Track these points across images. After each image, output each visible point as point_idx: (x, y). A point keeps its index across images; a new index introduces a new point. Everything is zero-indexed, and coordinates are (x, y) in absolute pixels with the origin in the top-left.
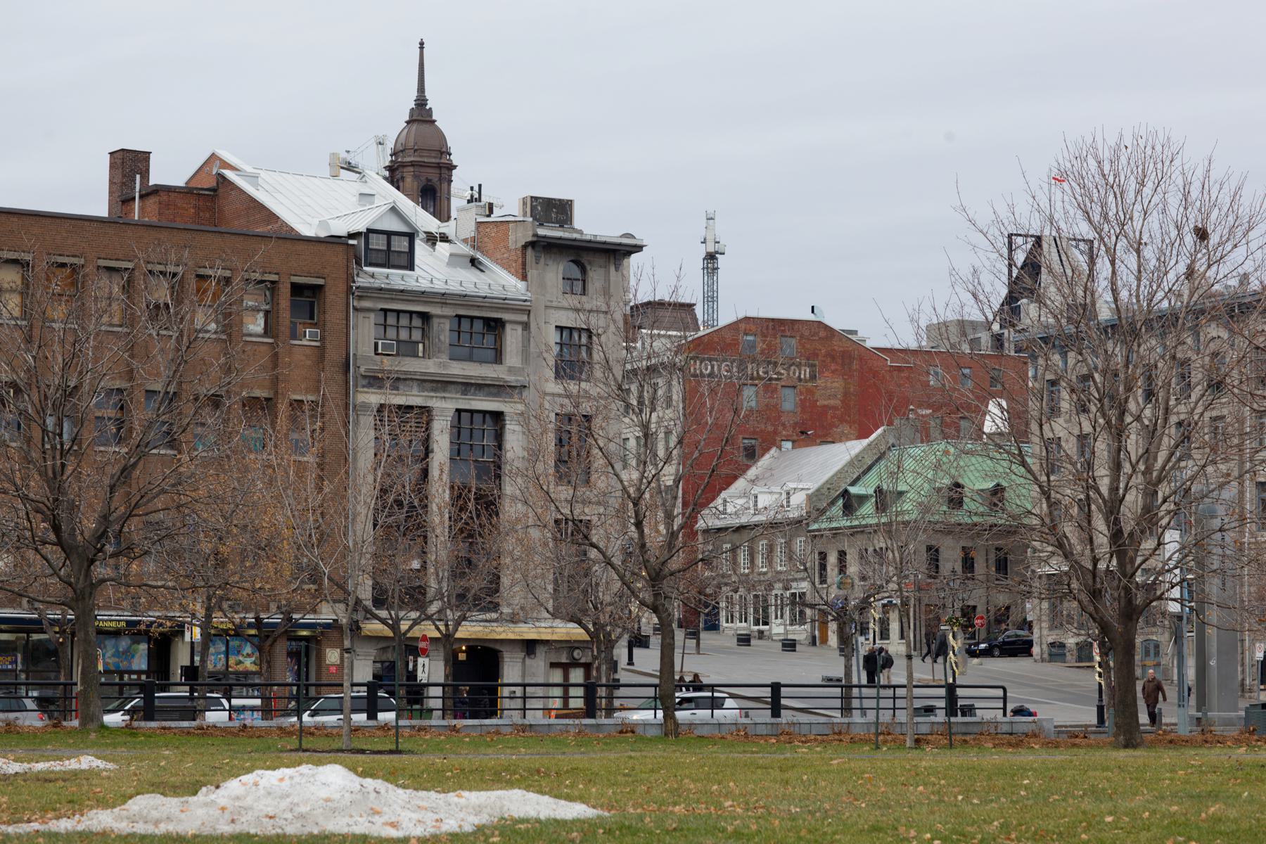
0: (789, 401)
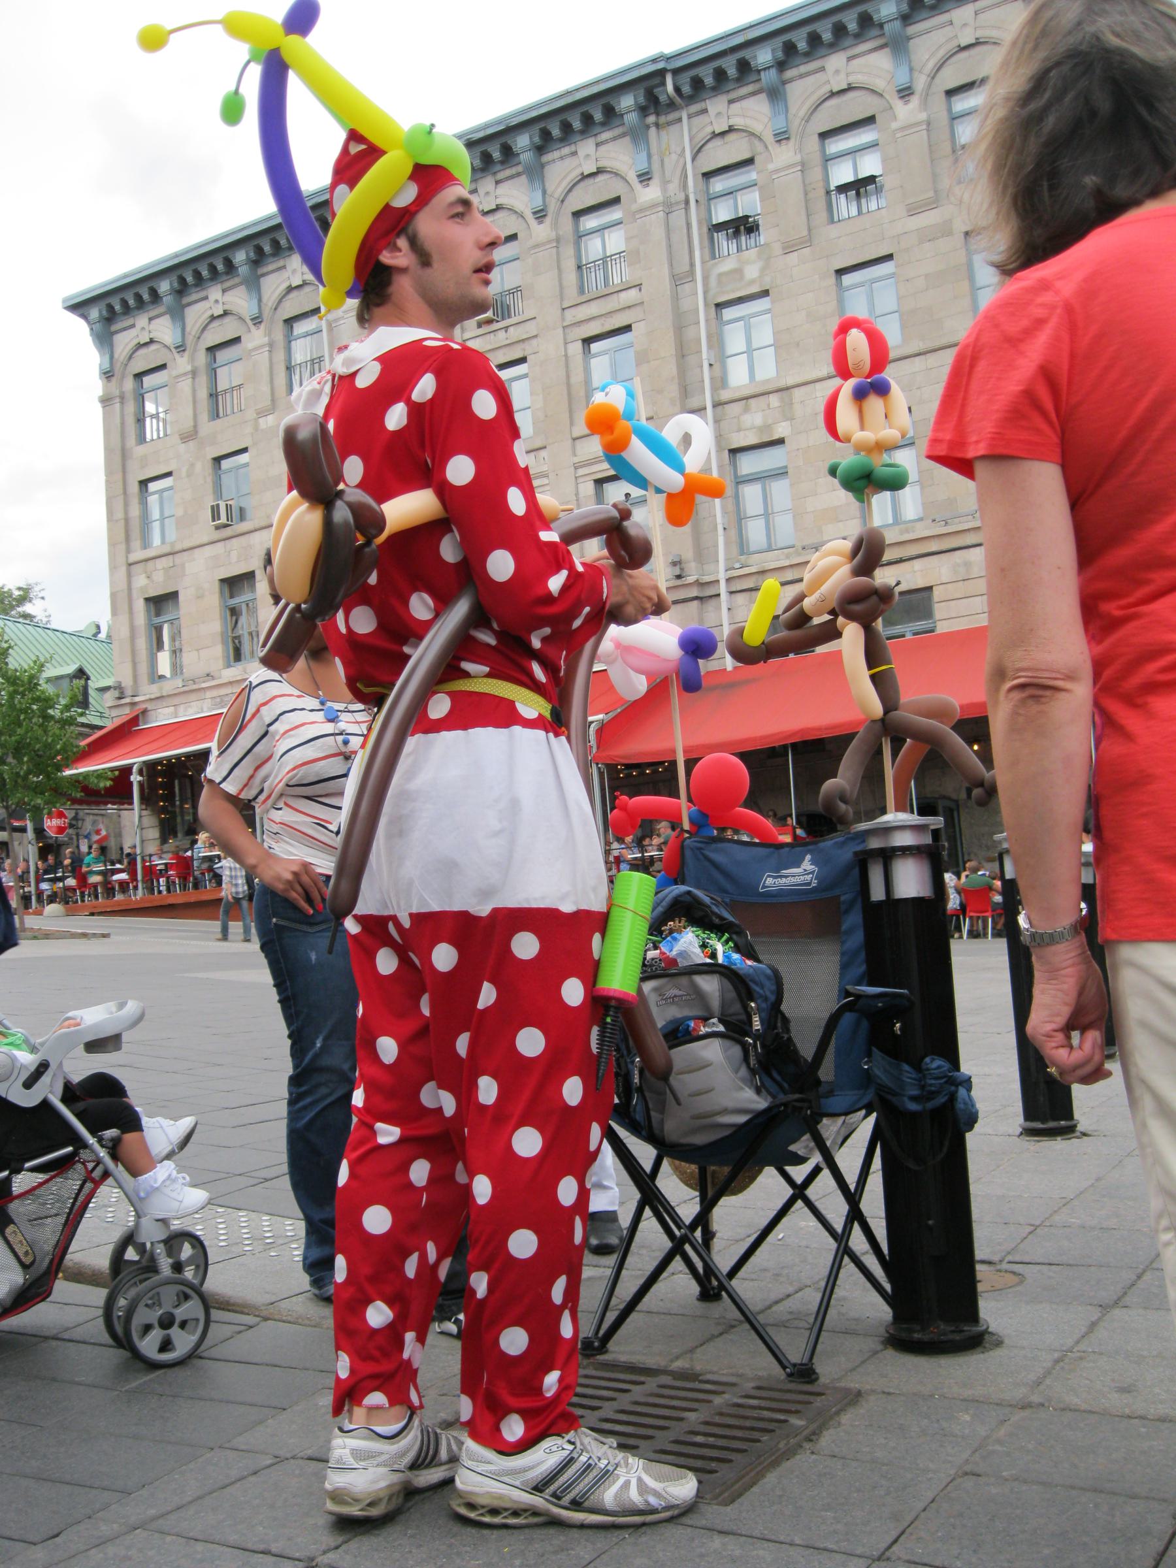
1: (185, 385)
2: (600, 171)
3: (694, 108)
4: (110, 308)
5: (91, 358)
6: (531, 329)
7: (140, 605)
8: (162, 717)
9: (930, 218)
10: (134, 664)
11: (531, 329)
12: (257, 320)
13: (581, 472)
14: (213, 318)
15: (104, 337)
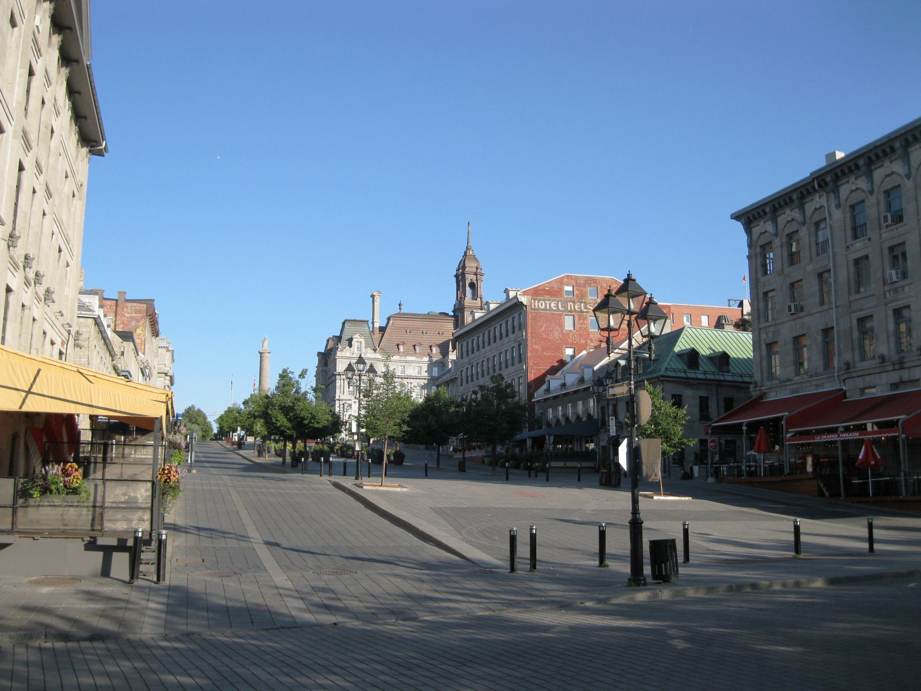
1: (778, 251)
4: (749, 218)
5: (744, 237)
7: (764, 346)
8: (772, 397)
10: (762, 374)
12: (804, 223)
14: (788, 222)
15: (748, 230)
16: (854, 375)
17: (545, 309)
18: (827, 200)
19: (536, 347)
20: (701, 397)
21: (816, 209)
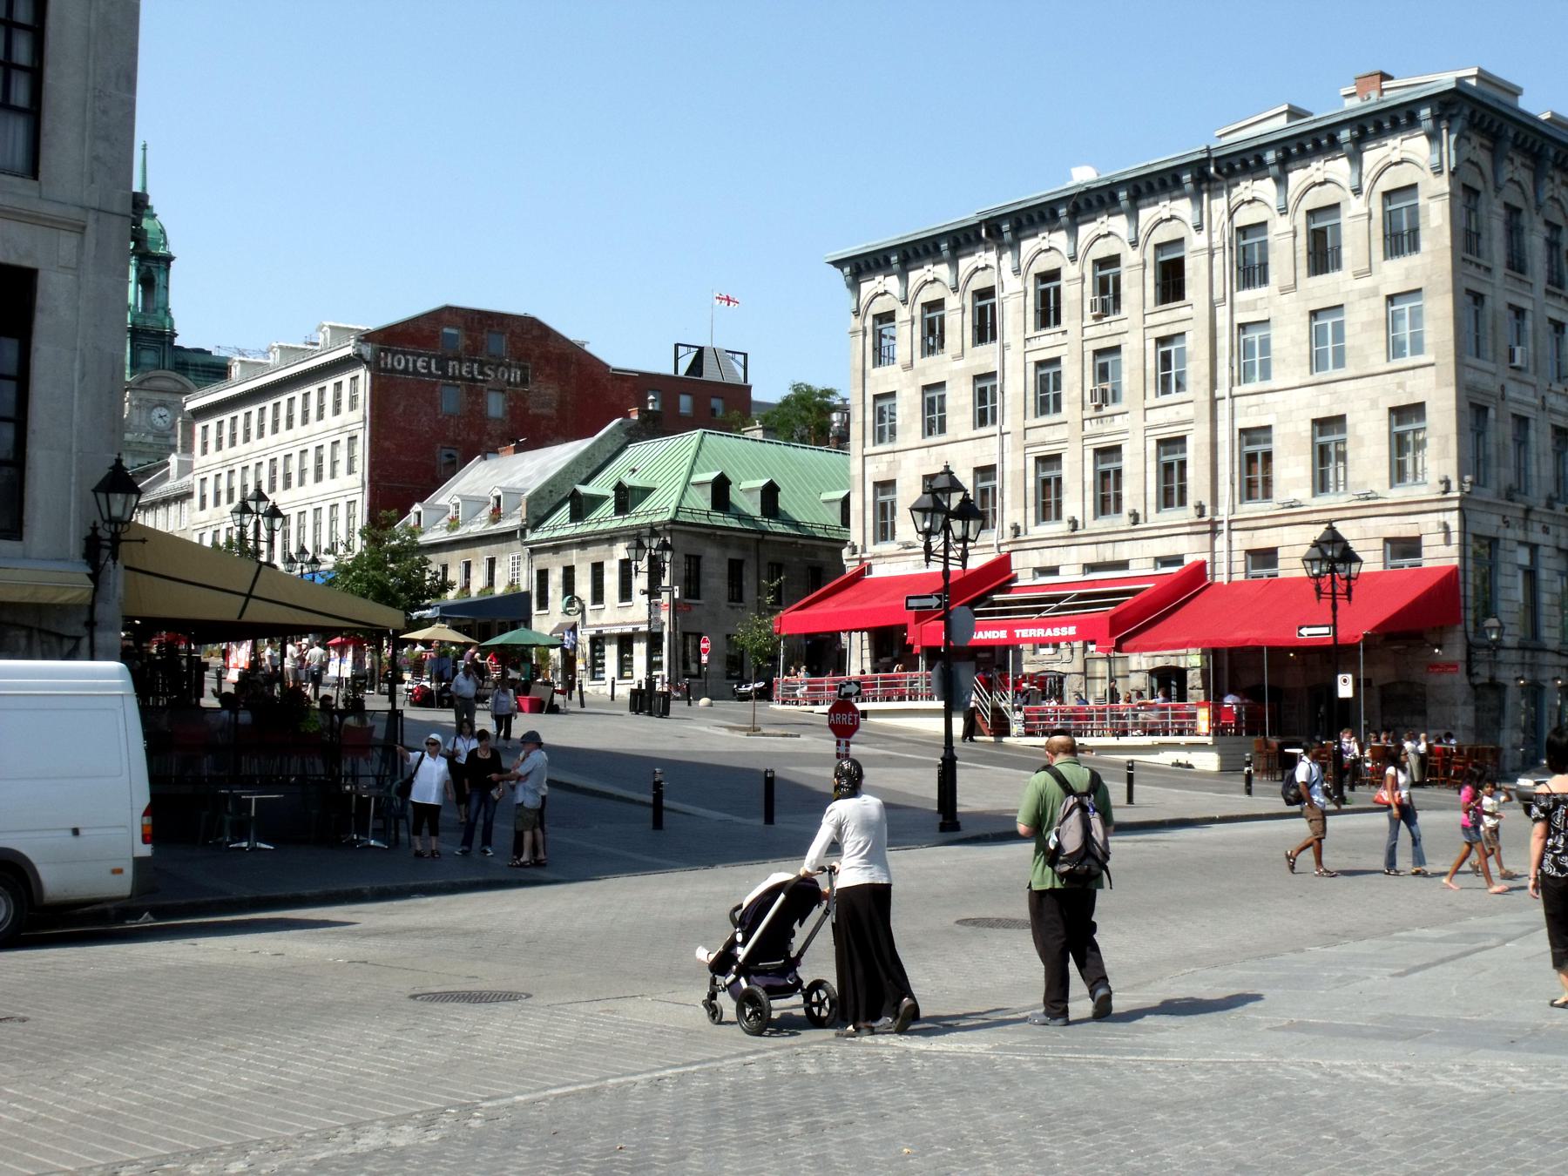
0: (496, 406)
2: (1172, 218)
3: (1232, 181)
6: (1124, 325)
8: (880, 571)
9: (1366, 283)
11: (1124, 325)
13: (1149, 433)
14: (926, 282)
15: (854, 286)
16: (1027, 545)
17: (405, 371)
18: (999, 258)
19: (387, 444)
20: (731, 562)
21: (977, 269)
